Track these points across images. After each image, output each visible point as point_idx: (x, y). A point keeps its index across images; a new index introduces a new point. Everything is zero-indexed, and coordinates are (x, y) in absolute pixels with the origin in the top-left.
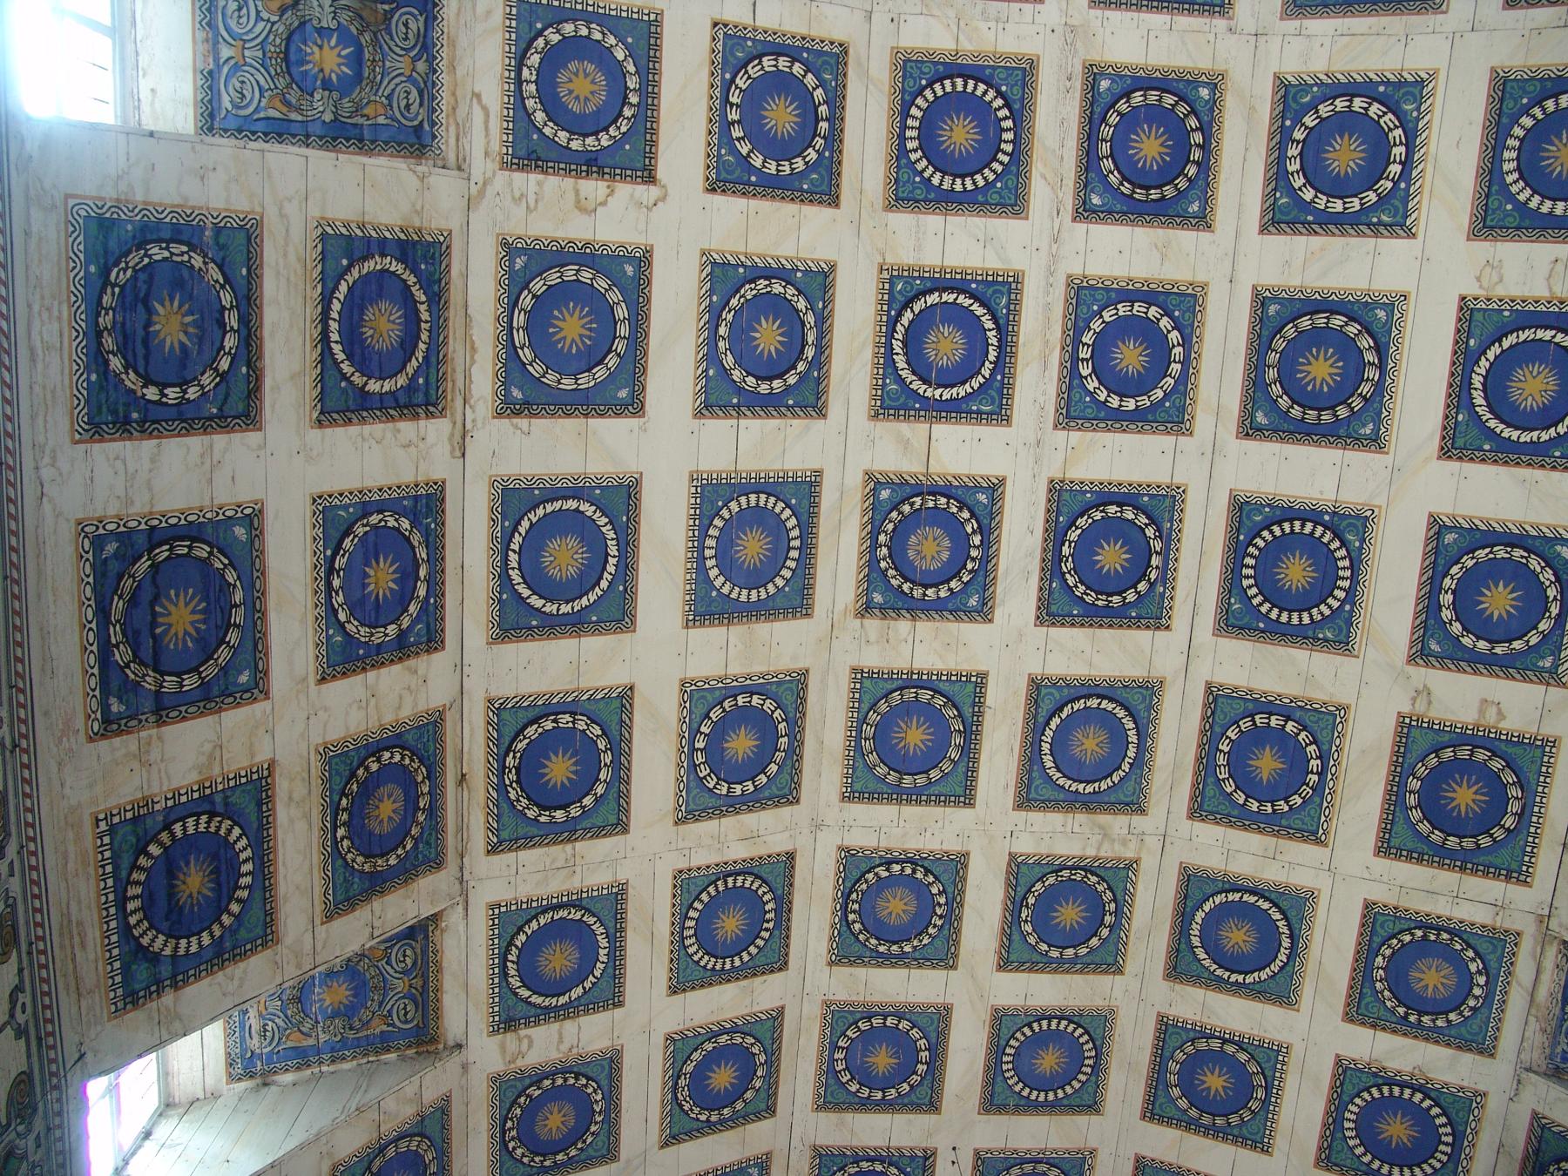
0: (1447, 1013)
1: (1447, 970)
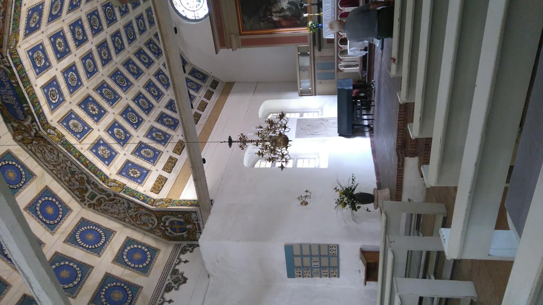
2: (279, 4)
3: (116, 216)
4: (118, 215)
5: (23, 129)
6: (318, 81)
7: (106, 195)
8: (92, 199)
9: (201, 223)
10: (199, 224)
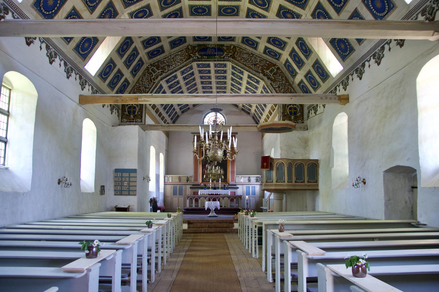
3: (141, 79)
4: (141, 80)
5: (194, 51)
6: (172, 186)
7: (154, 78)
8: (152, 70)
9: (134, 123)
10: (133, 122)
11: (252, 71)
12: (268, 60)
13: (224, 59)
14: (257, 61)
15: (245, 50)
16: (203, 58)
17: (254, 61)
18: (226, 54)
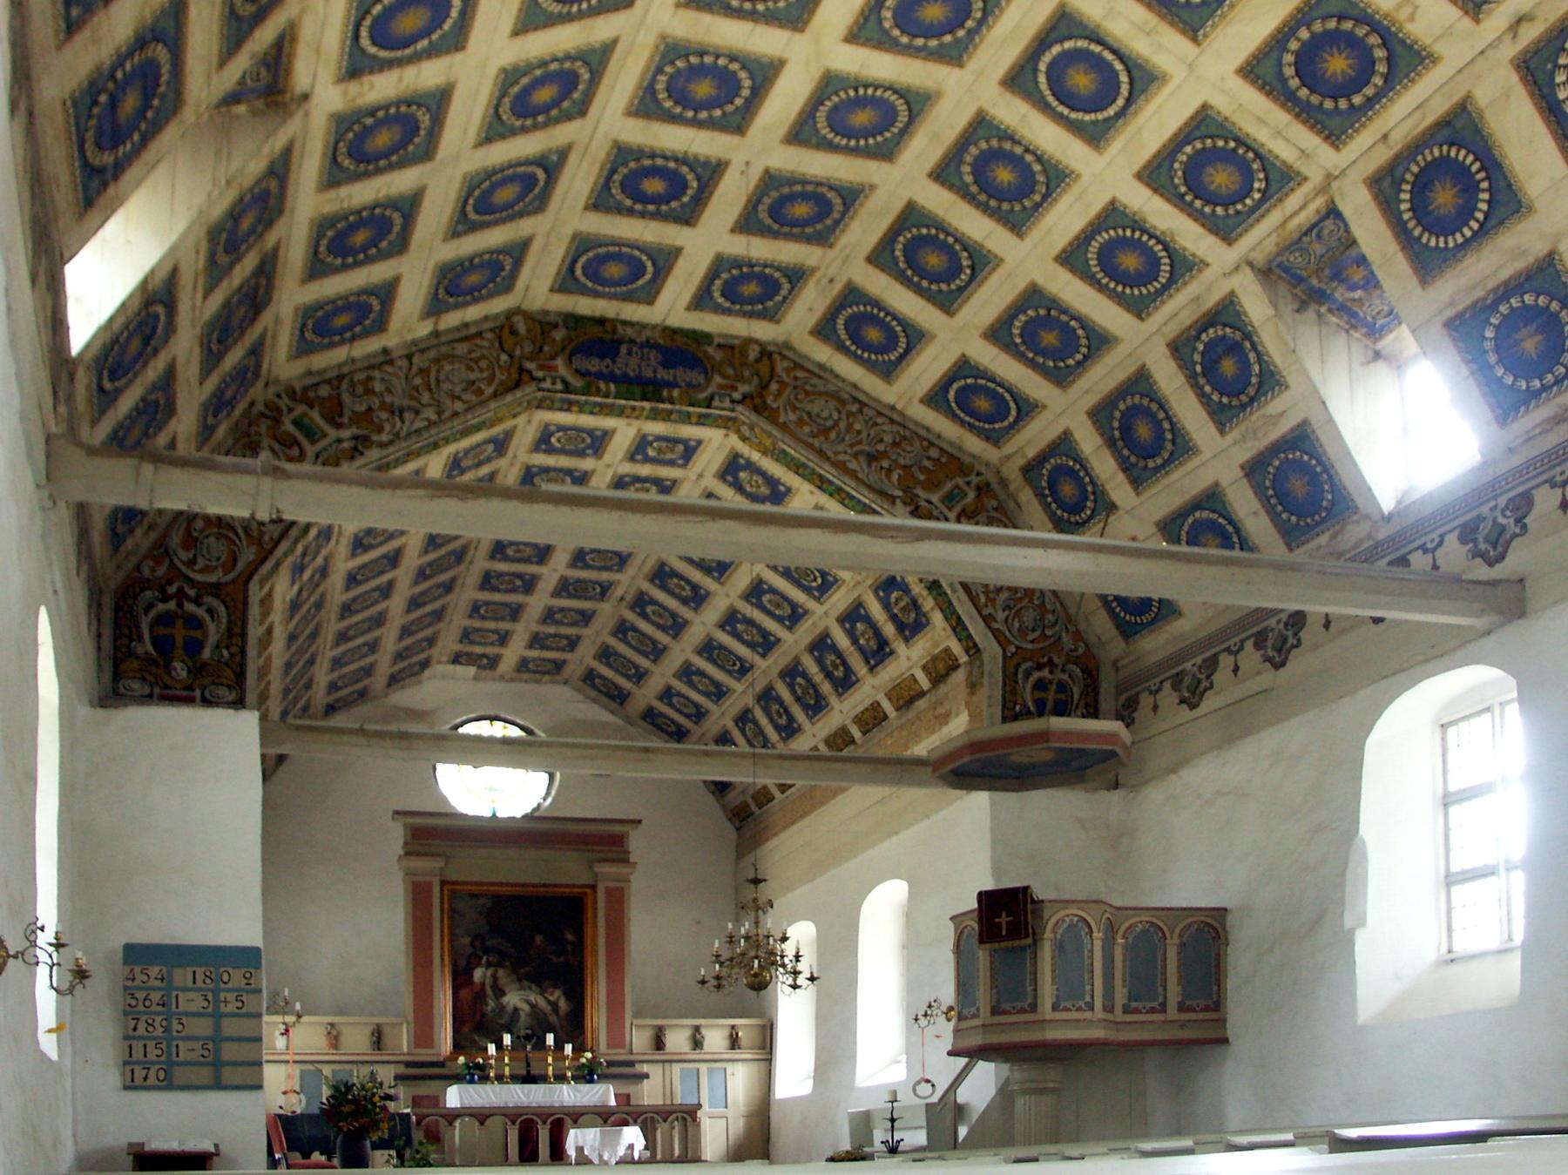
0: (1216, 205)
1: (1237, 178)
2: (513, 986)
11: (853, 484)
12: (933, 439)
13: (709, 407)
14: (881, 440)
15: (822, 374)
16: (594, 389)
17: (864, 436)
18: (721, 387)
